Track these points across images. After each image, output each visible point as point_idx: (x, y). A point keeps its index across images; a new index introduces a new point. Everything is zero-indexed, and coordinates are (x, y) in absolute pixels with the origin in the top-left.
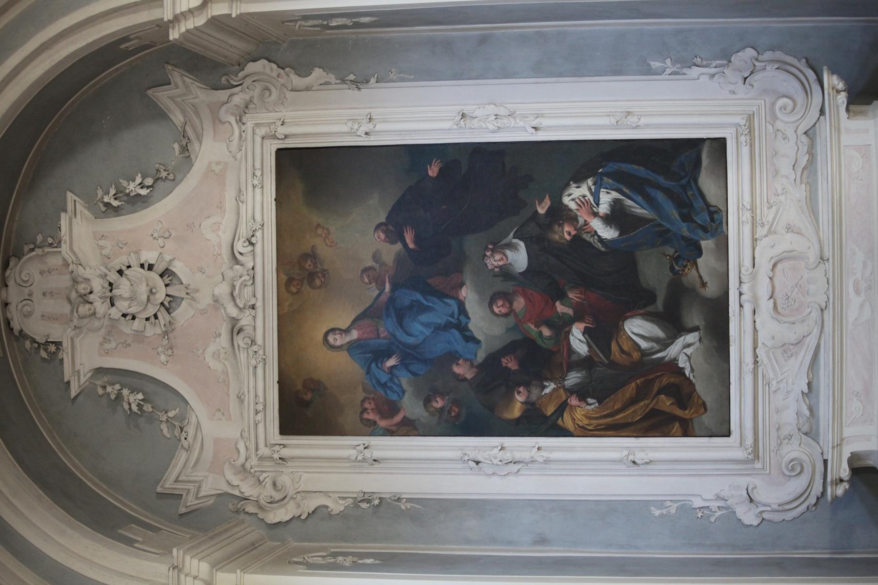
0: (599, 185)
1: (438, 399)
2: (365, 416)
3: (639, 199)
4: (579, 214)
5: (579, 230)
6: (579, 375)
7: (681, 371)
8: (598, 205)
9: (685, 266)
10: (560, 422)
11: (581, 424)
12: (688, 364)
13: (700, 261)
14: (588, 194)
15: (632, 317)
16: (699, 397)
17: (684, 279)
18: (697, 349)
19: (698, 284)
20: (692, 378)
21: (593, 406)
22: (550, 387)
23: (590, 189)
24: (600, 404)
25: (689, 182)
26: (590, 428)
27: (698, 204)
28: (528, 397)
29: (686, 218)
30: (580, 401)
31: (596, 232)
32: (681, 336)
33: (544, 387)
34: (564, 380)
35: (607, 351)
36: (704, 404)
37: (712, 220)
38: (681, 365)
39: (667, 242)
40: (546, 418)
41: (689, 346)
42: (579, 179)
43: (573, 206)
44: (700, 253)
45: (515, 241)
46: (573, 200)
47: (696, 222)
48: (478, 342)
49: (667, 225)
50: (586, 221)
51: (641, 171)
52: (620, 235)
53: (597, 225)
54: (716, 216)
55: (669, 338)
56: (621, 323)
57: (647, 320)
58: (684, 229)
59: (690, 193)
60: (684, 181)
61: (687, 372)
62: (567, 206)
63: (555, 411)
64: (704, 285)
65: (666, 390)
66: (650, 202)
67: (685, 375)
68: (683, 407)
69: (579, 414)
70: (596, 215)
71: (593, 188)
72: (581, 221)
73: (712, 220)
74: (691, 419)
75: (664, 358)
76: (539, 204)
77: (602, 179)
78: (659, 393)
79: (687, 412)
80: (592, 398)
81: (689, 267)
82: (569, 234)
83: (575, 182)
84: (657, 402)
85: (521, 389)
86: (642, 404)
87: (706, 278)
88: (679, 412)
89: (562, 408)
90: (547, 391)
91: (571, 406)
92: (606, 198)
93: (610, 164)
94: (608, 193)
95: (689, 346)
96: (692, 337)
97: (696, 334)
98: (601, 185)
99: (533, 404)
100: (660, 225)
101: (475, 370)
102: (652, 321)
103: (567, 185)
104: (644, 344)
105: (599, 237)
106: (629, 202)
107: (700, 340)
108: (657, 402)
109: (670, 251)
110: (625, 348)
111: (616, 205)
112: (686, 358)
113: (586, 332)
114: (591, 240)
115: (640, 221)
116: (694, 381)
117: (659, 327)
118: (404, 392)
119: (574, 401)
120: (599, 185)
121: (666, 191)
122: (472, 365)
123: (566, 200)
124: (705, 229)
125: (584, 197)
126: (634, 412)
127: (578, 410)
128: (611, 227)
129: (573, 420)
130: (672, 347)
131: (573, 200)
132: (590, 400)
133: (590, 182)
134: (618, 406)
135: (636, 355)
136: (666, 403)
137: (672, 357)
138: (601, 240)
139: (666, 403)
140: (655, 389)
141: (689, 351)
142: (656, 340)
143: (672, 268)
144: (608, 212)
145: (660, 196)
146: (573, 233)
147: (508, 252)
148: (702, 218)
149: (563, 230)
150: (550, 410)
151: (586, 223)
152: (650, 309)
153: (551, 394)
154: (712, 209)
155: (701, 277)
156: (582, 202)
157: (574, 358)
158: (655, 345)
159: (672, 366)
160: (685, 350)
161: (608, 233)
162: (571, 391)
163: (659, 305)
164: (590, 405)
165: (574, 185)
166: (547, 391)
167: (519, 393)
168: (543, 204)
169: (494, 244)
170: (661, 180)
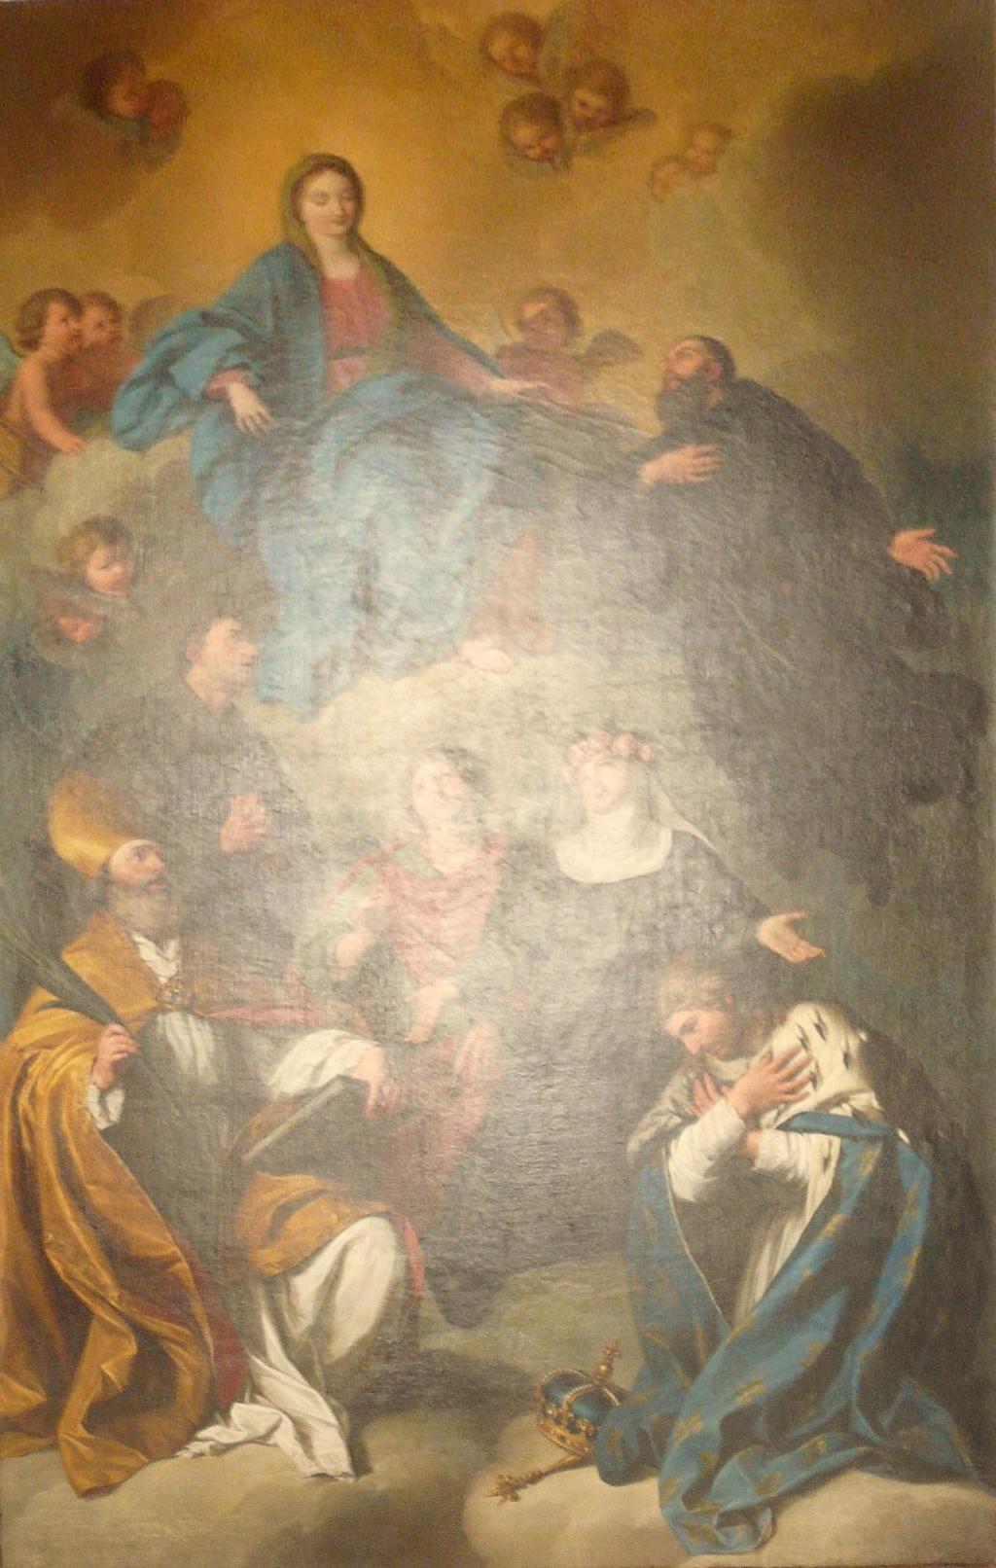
0: (851, 1131)
1: (117, 569)
2: (56, 310)
3: (805, 1270)
4: (755, 1061)
5: (701, 1065)
6: (203, 1061)
7: (216, 1408)
8: (785, 1127)
9: (573, 1428)
10: (43, 996)
11: (34, 1069)
12: (241, 1436)
13: (590, 1475)
14: (825, 1091)
15: (402, 1247)
16: (131, 1472)
17: (529, 1420)
18: (294, 1468)
19: (514, 1470)
20: (195, 1447)
21: (95, 1109)
22: (161, 962)
23: (841, 1099)
24: (105, 1133)
25: (859, 1439)
26: (23, 1101)
27: (783, 1469)
28: (127, 887)
29: (737, 1430)
30: (116, 1066)
31: (690, 1119)
32: (336, 1411)
33: (159, 940)
34: (187, 1009)
35: (283, 1162)
36: (107, 1488)
37: (728, 1519)
38: (238, 1410)
39: (655, 1368)
40: (55, 952)
41: (304, 1438)
42: (880, 1061)
43: (783, 1040)
44: (619, 1474)
45: (665, 838)
46: (804, 1042)
47: (718, 1467)
48: (316, 703)
49: (712, 1366)
50: (730, 1084)
51: (900, 1274)
52: (680, 1204)
53: (719, 1122)
54: (740, 1531)
55: (329, 1371)
56: (381, 1207)
57: (391, 1299)
58: (700, 1423)
59: (821, 1443)
60: (861, 1423)
61: (214, 1433)
62: (783, 1020)
63: (76, 979)
64: (510, 1489)
65: (153, 1358)
66: (793, 1309)
67: (206, 1421)
68: (99, 1416)
69: (67, 1062)
70: (753, 1119)
71: (844, 1110)
72: (730, 1069)
73: (728, 1519)
74: (55, 1446)
75: (261, 1350)
76: (794, 925)
77: (872, 1140)
78: (139, 1331)
79: (82, 1431)
80: (125, 1111)
81: (571, 1438)
82: (689, 1028)
83: (864, 1047)
84: (110, 1330)
85: (152, 861)
86: (106, 1278)
87: (530, 1495)
88: (78, 1404)
89: (94, 1008)
90: (148, 952)
91: (95, 1037)
92: (807, 1158)
93: (923, 1170)
94: (826, 1162)
95: (304, 1438)
96: (331, 1449)
97: (344, 1465)
98: (854, 1139)
99: (103, 902)
100: (713, 1340)
101: (219, 698)
102: (385, 1319)
103: (853, 1020)
104: (306, 1286)
105: (674, 1133)
106: (792, 1234)
107: (322, 1476)
108: (110, 1330)
109: (624, 1377)
110: (296, 1222)
111: (785, 1190)
112: (262, 1430)
113: (351, 1091)
114: (666, 1105)
115: (729, 1275)
116: (184, 1454)
117: (362, 1342)
118: (139, 447)
119: (113, 1044)
120: (851, 1131)
121: (829, 1363)
122: (233, 688)
123: (804, 1017)
124: (695, 1495)
125: (814, 1079)
126: (80, 1255)
127: (83, 1061)
128: (708, 1173)
129: (47, 1044)
130: (298, 1381)
131: (804, 1042)
132: (116, 1100)
133: (866, 1100)
134: (99, 1198)
135: (269, 1257)
136: (108, 1359)
137: (265, 1382)
138: (665, 1137)
139: (108, 1359)
140: (158, 1325)
141: (286, 1438)
142: (322, 1330)
143: (567, 1381)
144: (759, 1164)
145: (811, 1341)
146: (691, 1043)
147: (627, 812)
148: (735, 1486)
149: (708, 1006)
150: (82, 962)
151: (723, 1086)
152: (429, 1309)
153: (137, 966)
154: (765, 1519)
155: (536, 1478)
156: (792, 1076)
157: (261, 1045)
158: (307, 1322)
159: (232, 1384)
160: (287, 1425)
161: (687, 1166)
162: (145, 1035)
163: (447, 1339)
164: (102, 1101)
165: (854, 1045)
166: (148, 952)
167: (140, 853)
168: (791, 937)
169: (652, 765)
170: (867, 1345)
